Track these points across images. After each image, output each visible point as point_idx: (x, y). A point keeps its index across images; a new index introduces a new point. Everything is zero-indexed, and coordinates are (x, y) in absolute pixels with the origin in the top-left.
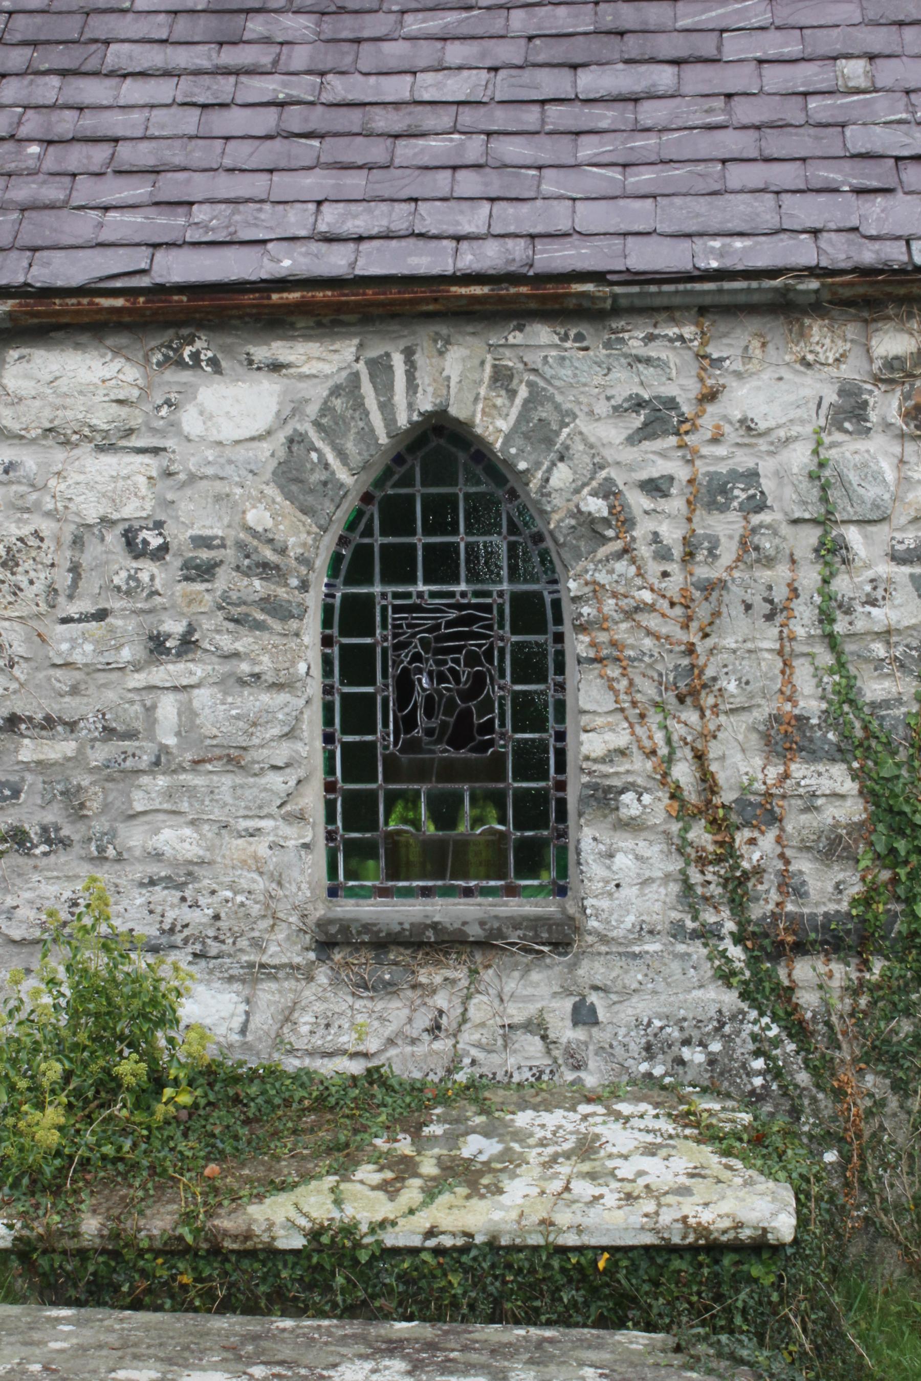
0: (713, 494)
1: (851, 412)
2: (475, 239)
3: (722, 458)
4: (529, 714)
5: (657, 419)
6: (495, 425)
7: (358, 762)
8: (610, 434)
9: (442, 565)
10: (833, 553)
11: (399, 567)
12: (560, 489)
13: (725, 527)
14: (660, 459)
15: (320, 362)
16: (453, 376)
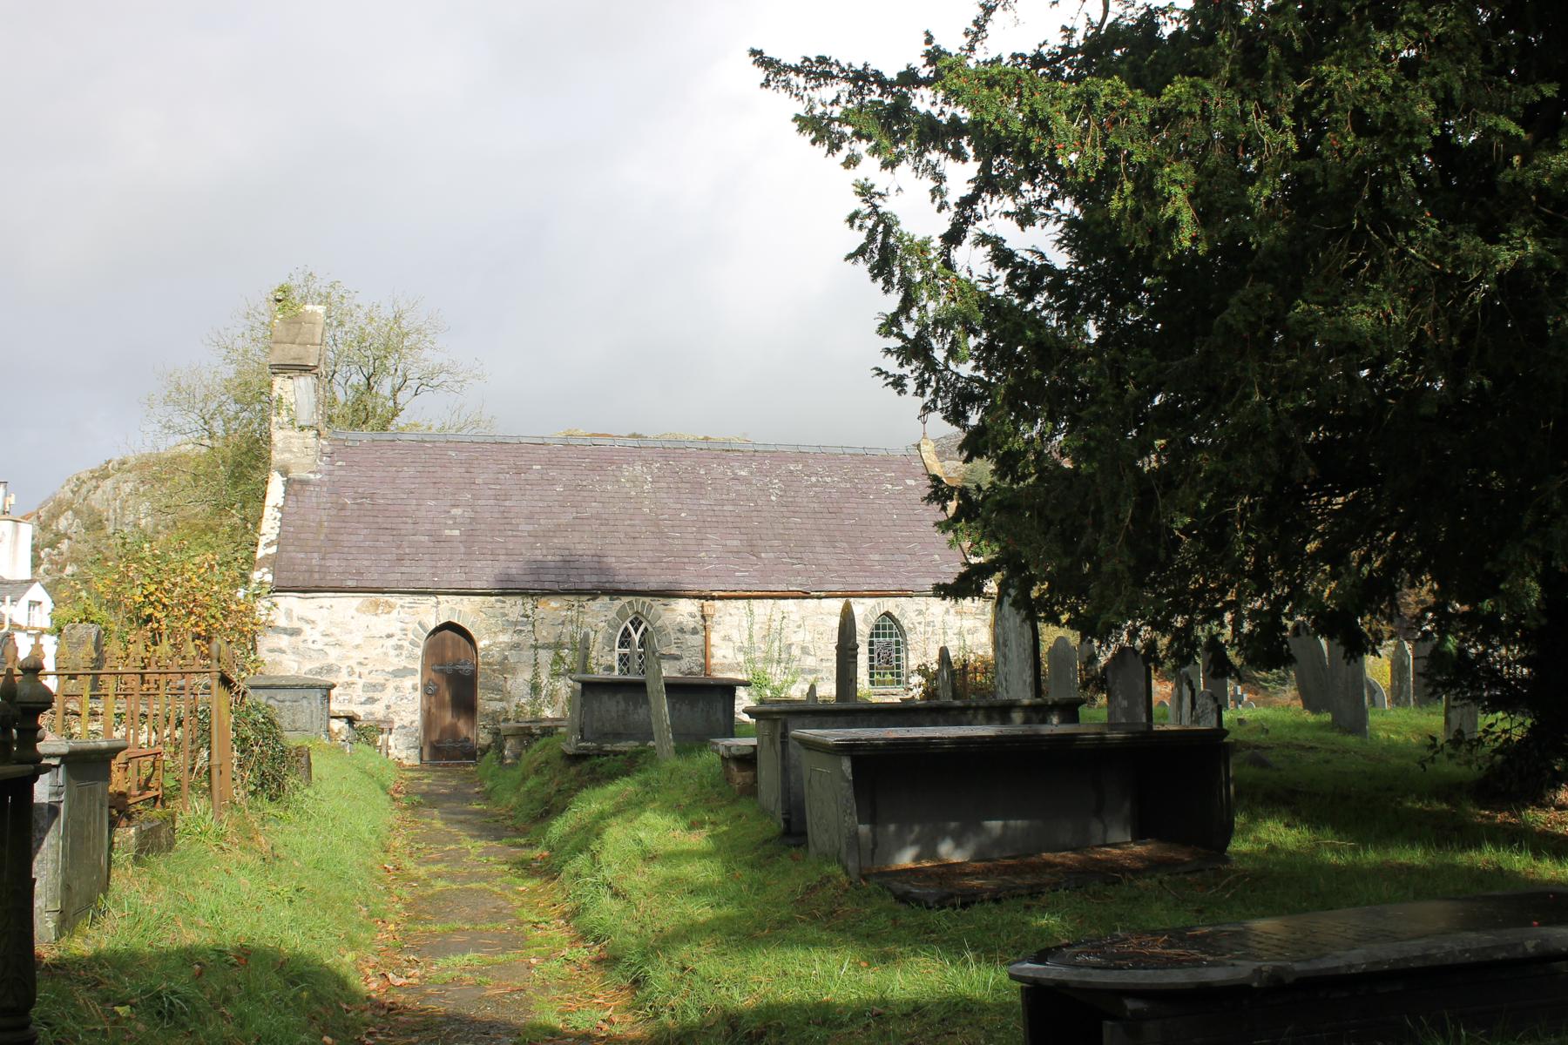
0: (928, 624)
1: (947, 612)
2: (890, 584)
3: (929, 619)
4: (898, 659)
5: (920, 613)
6: (896, 614)
7: (872, 667)
8: (913, 615)
9: (884, 635)
10: (945, 633)
11: (878, 636)
12: (905, 623)
13: (930, 629)
14: (920, 618)
15: (873, 601)
16: (889, 604)
